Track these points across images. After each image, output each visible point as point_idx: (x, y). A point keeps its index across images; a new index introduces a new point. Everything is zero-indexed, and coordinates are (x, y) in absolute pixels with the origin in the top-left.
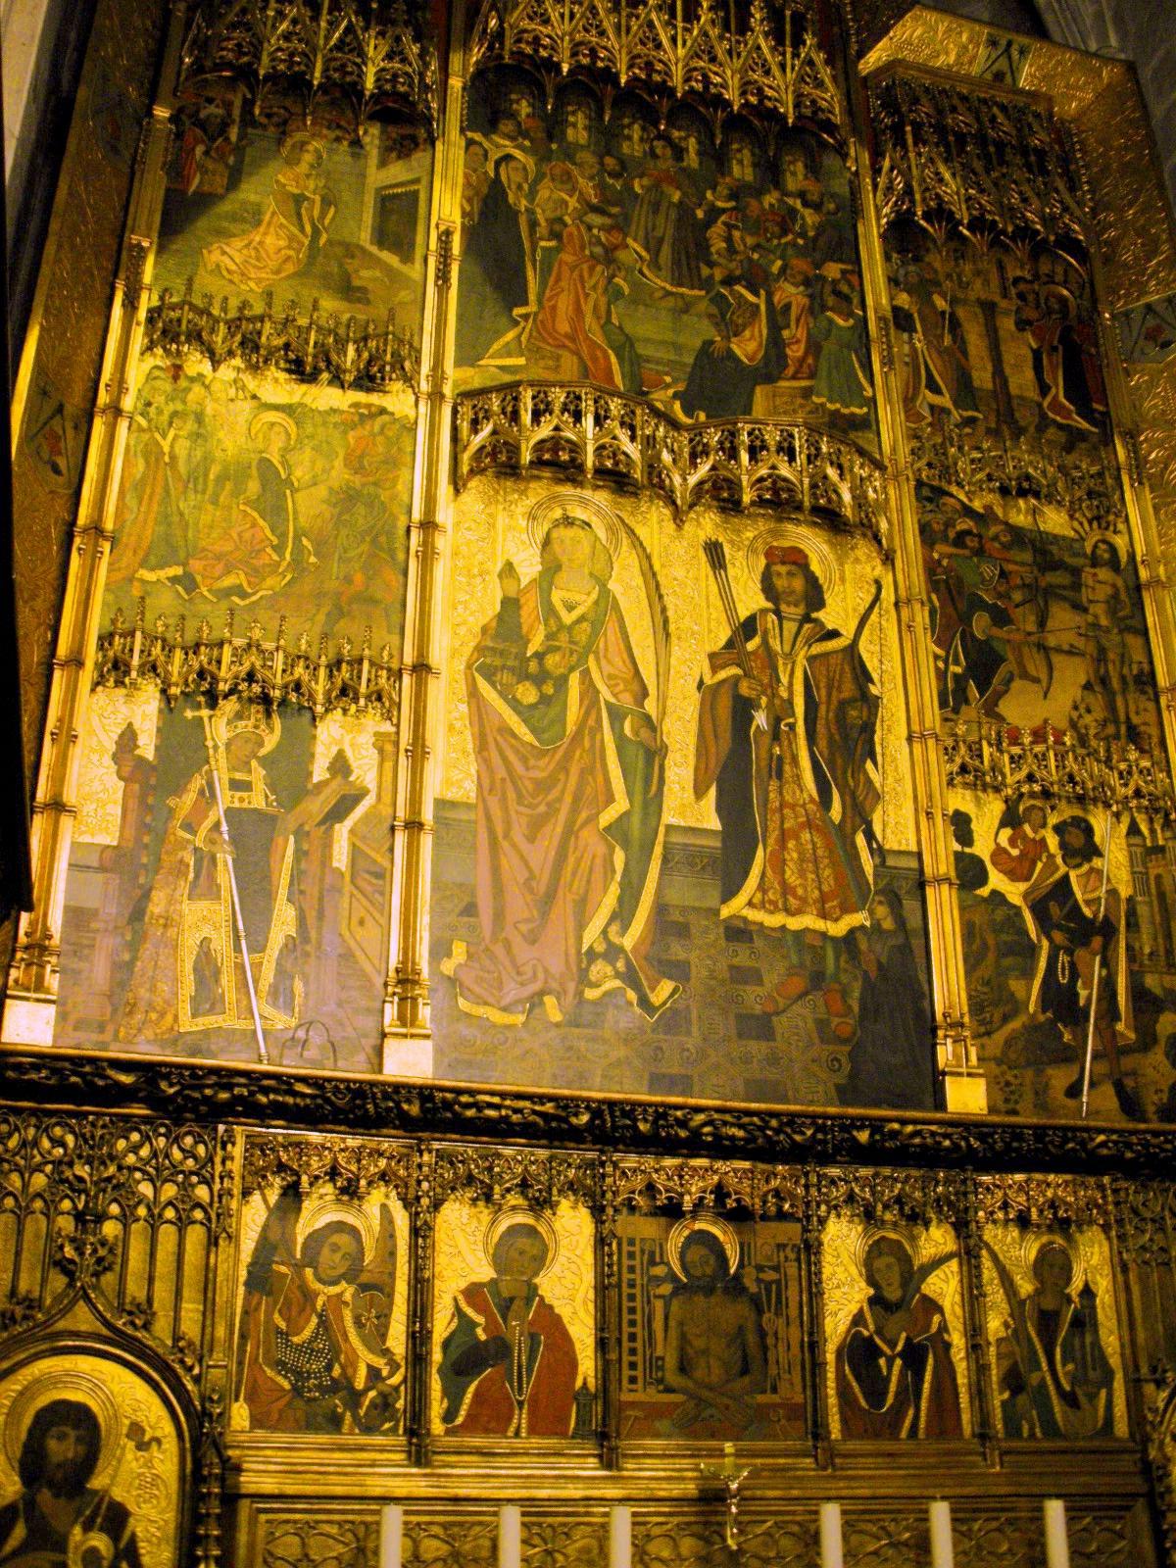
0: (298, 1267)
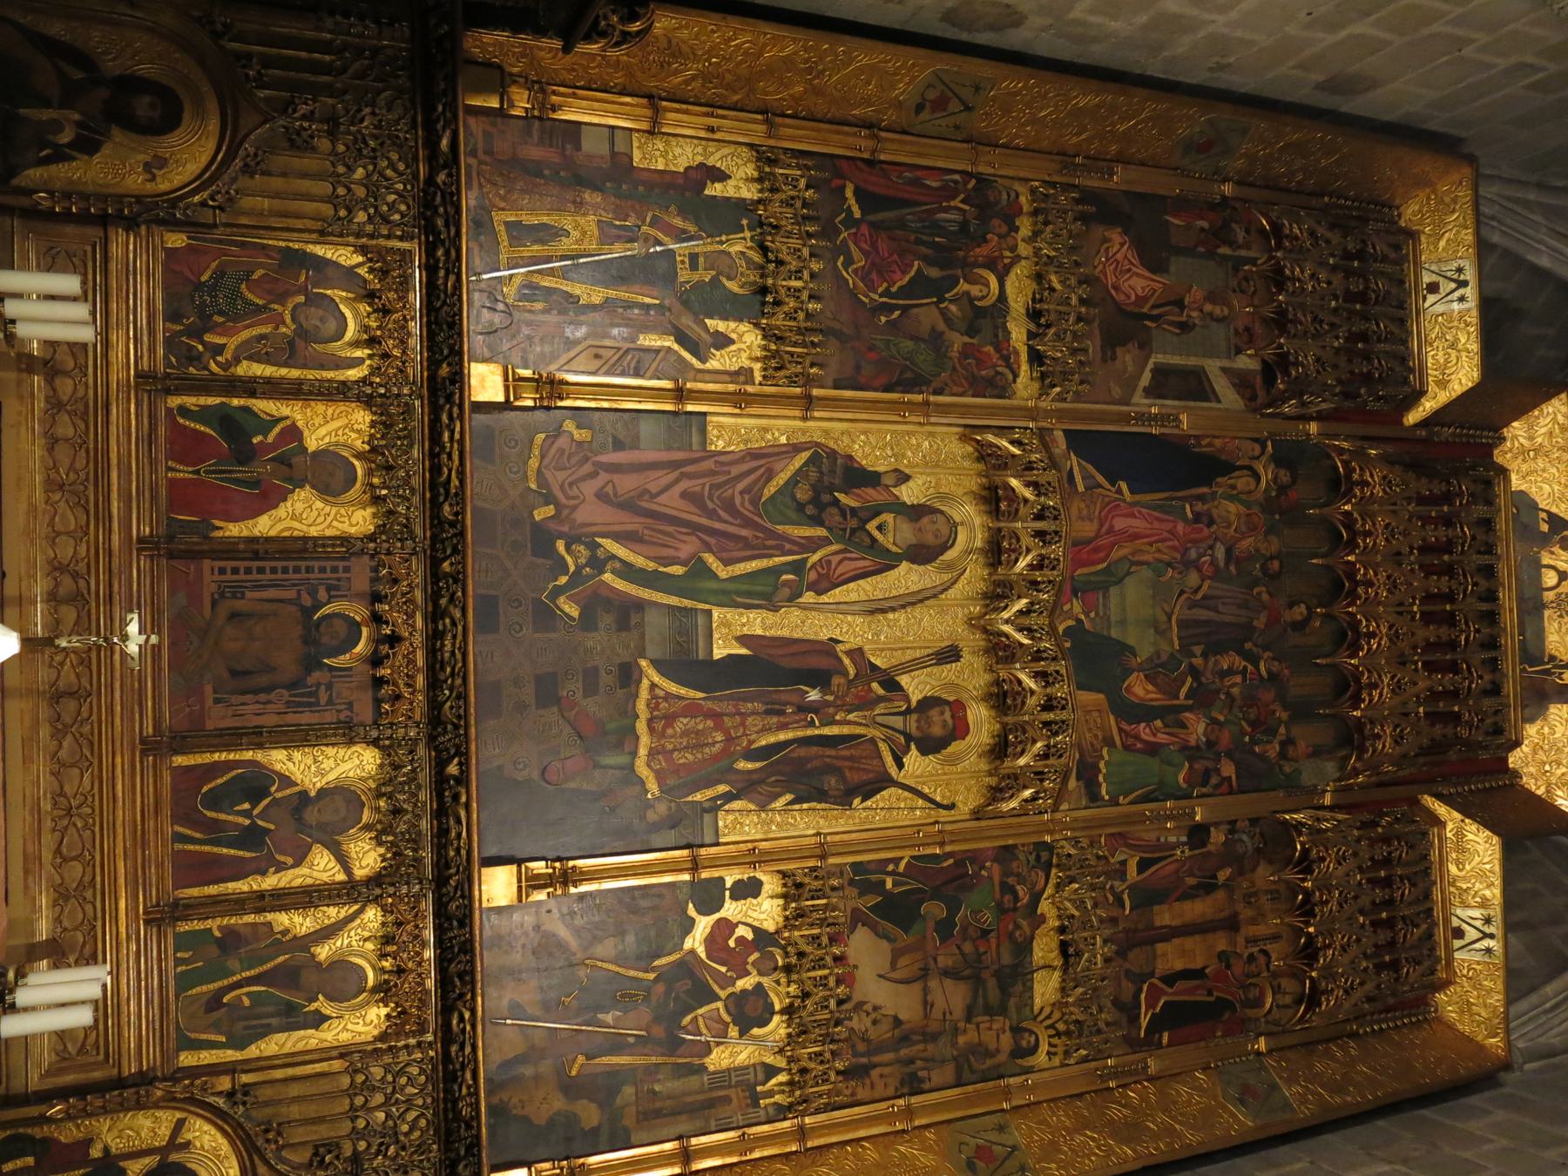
0: (304, 290)
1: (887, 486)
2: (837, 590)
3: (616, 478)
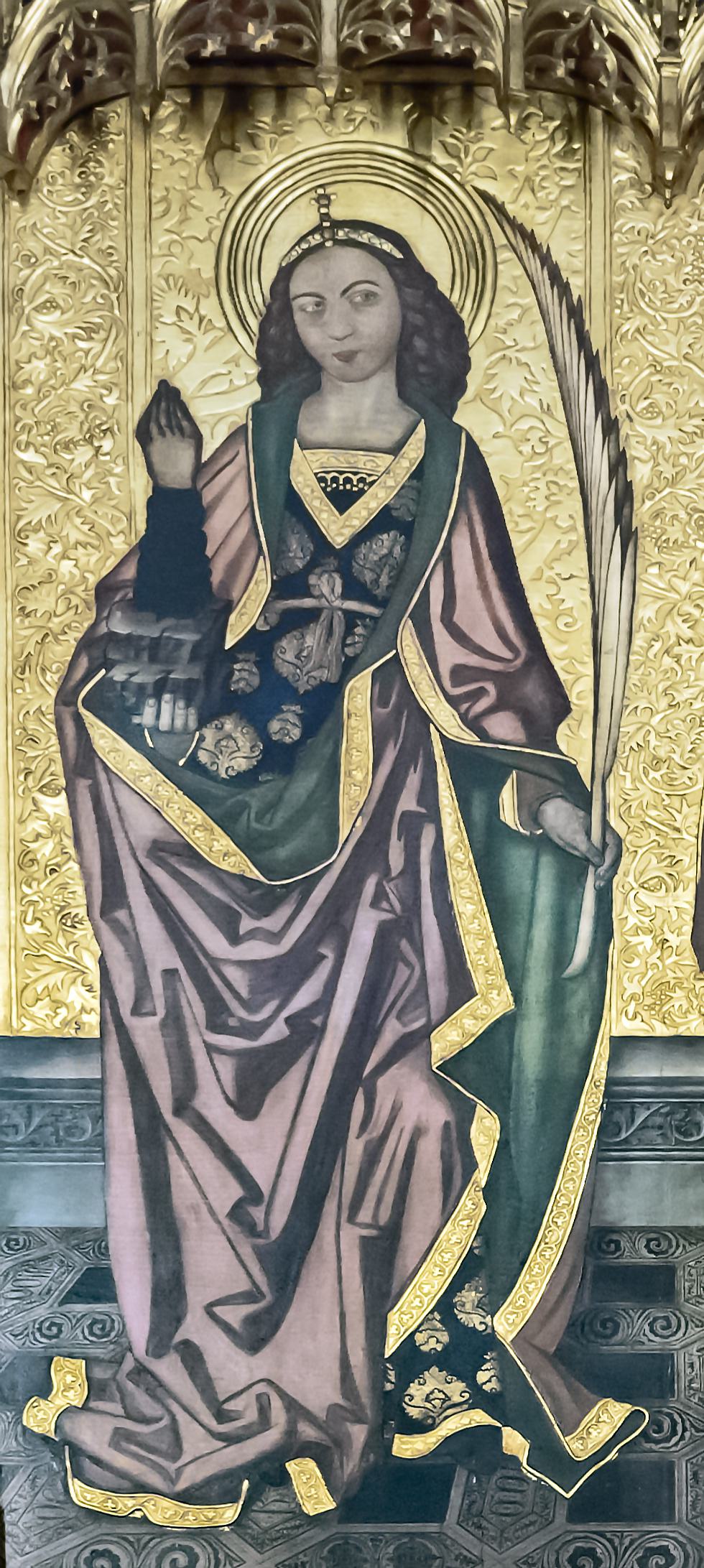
3: (197, 1297)
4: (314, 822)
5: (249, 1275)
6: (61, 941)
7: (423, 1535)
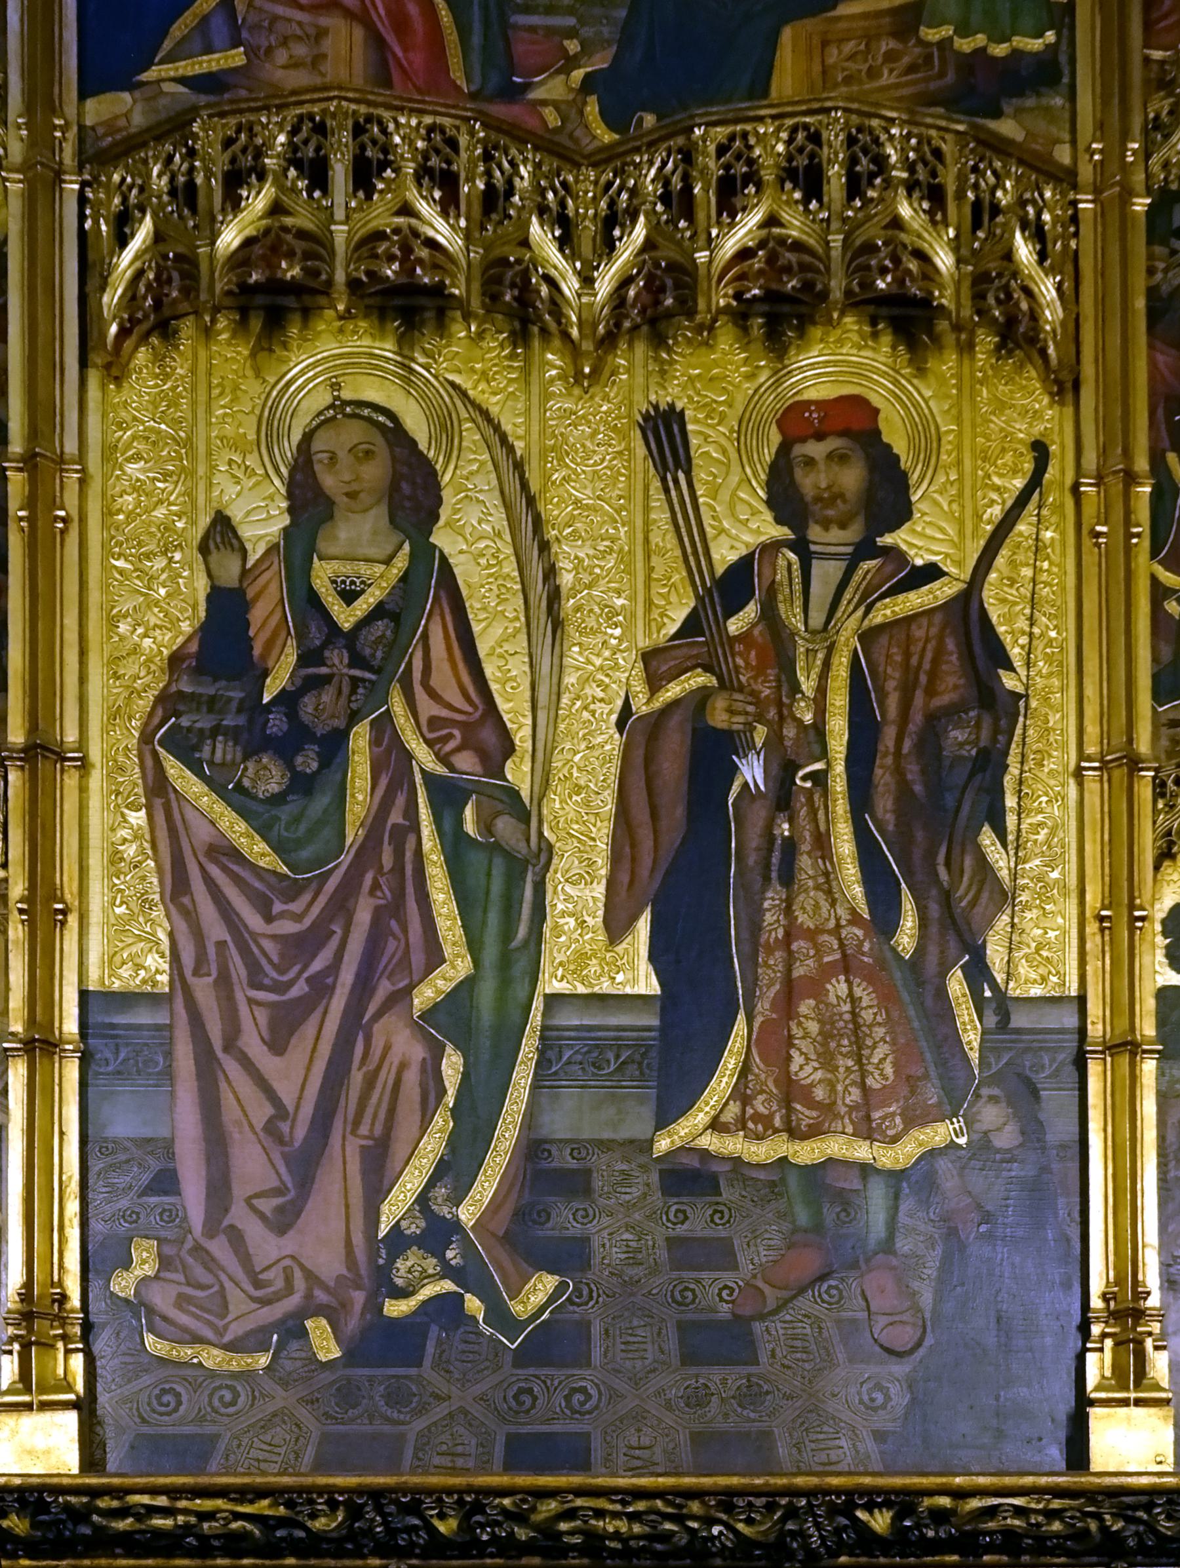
1: (244, 572)
2: (503, 706)
3: (240, 1191)
4: (327, 832)
5: (277, 1173)
6: (141, 919)
7: (406, 1377)
